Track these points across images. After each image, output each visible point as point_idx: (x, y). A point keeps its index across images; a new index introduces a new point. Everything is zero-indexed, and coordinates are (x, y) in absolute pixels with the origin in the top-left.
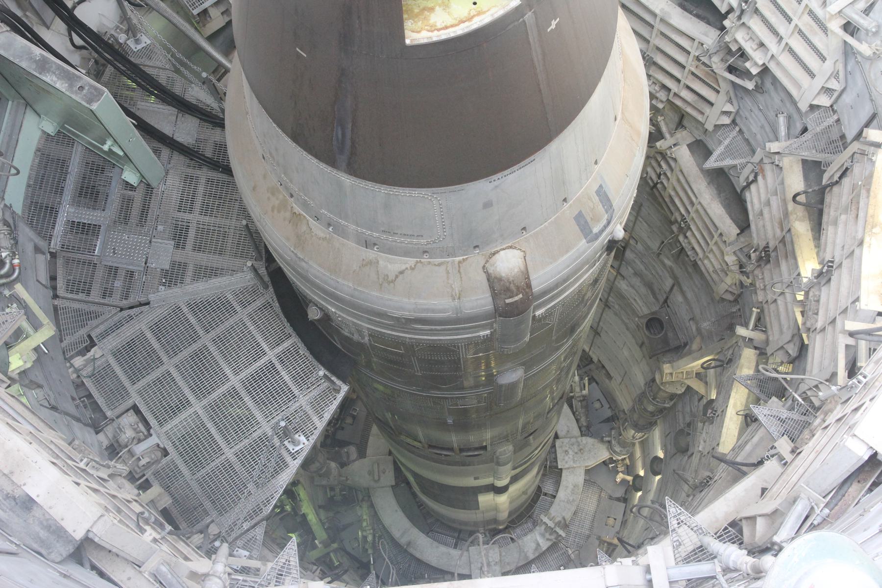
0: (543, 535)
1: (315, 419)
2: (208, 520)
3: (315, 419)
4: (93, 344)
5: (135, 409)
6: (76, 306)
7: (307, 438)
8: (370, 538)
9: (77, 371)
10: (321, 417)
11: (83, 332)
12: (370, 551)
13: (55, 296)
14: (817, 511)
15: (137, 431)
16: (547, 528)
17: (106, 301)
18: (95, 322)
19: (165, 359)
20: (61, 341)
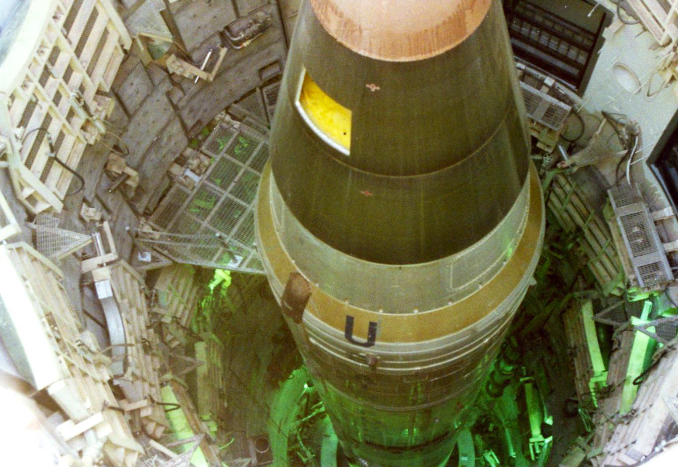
6: (260, 101)
11: (247, 112)
13: (261, 88)
15: (199, 167)
18: (254, 115)
19: (248, 163)
20: (236, 102)
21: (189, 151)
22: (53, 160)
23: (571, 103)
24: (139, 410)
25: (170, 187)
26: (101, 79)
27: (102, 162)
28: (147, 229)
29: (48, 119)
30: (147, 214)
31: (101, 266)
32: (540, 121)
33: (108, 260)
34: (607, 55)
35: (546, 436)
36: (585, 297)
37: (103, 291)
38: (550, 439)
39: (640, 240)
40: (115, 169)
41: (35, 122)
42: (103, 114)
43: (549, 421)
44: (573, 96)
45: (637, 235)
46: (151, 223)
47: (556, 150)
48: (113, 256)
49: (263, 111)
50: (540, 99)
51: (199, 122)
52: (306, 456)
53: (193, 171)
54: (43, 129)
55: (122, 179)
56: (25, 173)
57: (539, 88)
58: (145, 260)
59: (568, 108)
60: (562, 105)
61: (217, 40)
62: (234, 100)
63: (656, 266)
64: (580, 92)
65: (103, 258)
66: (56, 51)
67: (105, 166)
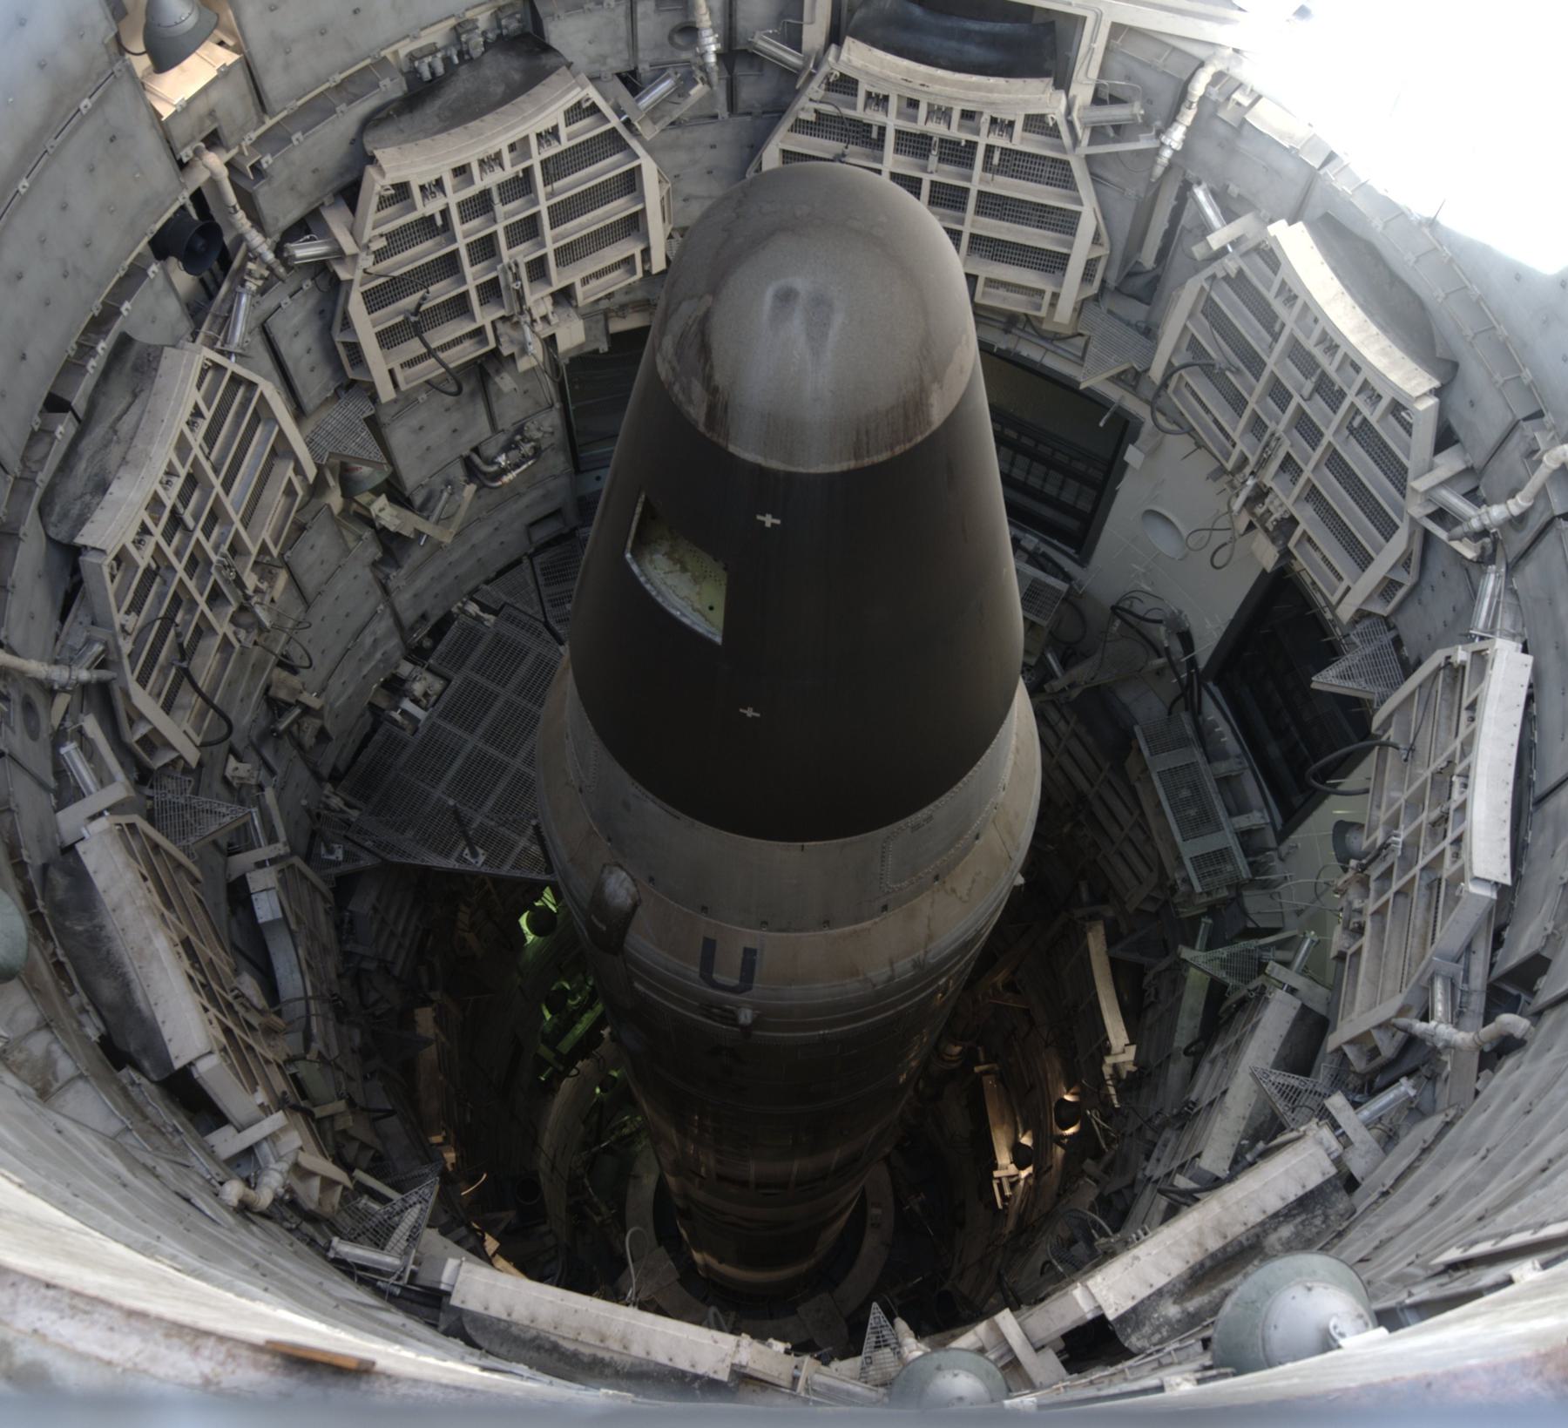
1: (510, 862)
3: (510, 862)
4: (495, 613)
5: (448, 681)
7: (485, 863)
8: (626, 1131)
9: (463, 611)
10: (513, 867)
12: (613, 1138)
13: (531, 557)
14: (392, 1280)
15: (426, 695)
17: (547, 605)
20: (487, 582)
21: (406, 669)
23: (1067, 577)
25: (374, 730)
28: (336, 802)
30: (335, 778)
31: (260, 865)
33: (273, 855)
34: (1129, 496)
35: (1021, 1167)
36: (1093, 917)
37: (266, 908)
38: (1030, 1170)
39: (1192, 812)
43: (1026, 1140)
44: (1068, 565)
48: (280, 848)
49: (534, 596)
51: (424, 617)
52: (599, 1214)
53: (416, 701)
58: (333, 857)
59: (1062, 586)
60: (1052, 581)
61: (458, 472)
62: (482, 578)
63: (1222, 855)
64: (1083, 559)
65: (265, 852)
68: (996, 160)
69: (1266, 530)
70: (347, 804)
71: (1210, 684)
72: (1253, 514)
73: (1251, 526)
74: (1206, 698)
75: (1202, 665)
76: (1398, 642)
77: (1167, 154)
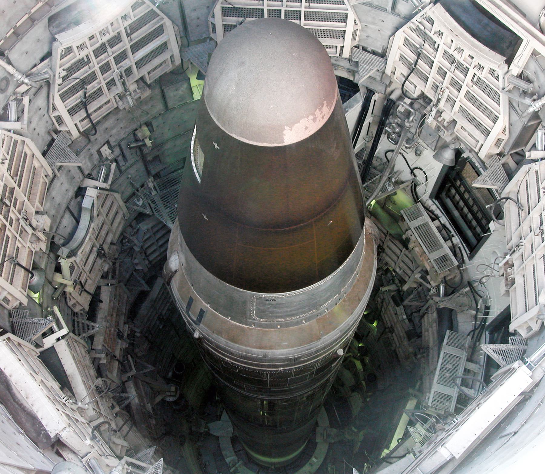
0: (233, 460)
2: (158, 190)
16: (236, 463)
22: (84, 105)
24: (66, 286)
26: (146, 73)
27: (134, 126)
28: (151, 185)
29: (93, 77)
30: (157, 176)
31: (97, 188)
32: (432, 261)
33: (101, 186)
36: (415, 396)
37: (87, 203)
39: (448, 375)
40: (139, 135)
41: (81, 74)
42: (138, 96)
44: (466, 257)
45: (448, 370)
46: (155, 184)
47: (438, 288)
48: (105, 186)
50: (442, 247)
54: (84, 83)
55: (140, 144)
56: (58, 102)
57: (445, 240)
58: (138, 203)
59: (456, 263)
63: (448, 398)
64: (471, 257)
66: (117, 39)
67: (136, 130)
68: (475, 80)
69: (507, 279)
70: (155, 187)
71: (487, 332)
72: (506, 271)
73: (503, 275)
74: (483, 336)
75: (487, 324)
76: (524, 352)
77: (531, 110)
